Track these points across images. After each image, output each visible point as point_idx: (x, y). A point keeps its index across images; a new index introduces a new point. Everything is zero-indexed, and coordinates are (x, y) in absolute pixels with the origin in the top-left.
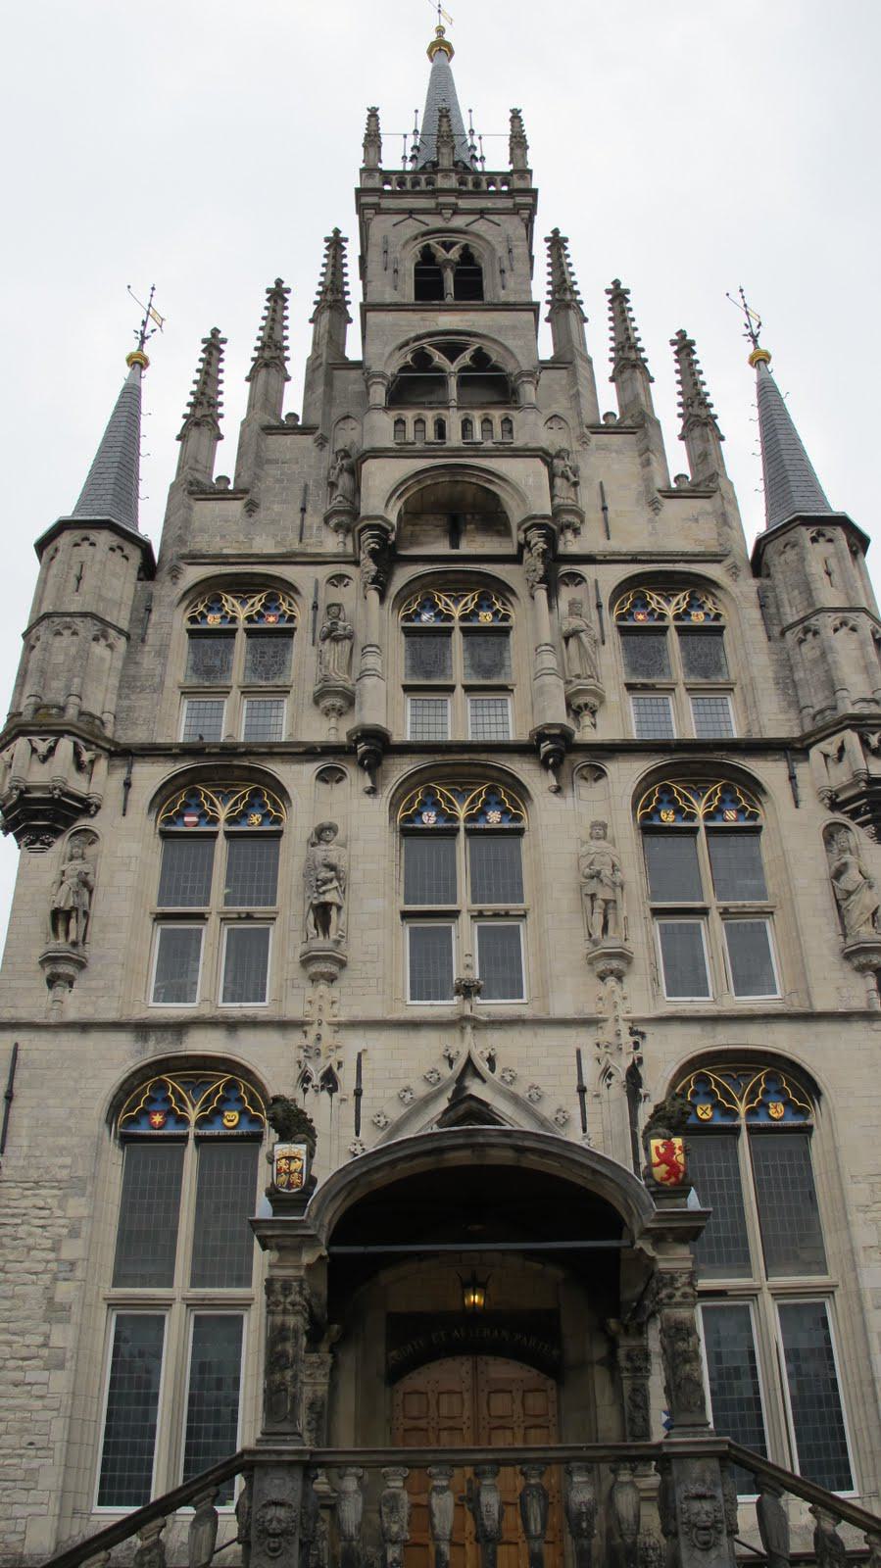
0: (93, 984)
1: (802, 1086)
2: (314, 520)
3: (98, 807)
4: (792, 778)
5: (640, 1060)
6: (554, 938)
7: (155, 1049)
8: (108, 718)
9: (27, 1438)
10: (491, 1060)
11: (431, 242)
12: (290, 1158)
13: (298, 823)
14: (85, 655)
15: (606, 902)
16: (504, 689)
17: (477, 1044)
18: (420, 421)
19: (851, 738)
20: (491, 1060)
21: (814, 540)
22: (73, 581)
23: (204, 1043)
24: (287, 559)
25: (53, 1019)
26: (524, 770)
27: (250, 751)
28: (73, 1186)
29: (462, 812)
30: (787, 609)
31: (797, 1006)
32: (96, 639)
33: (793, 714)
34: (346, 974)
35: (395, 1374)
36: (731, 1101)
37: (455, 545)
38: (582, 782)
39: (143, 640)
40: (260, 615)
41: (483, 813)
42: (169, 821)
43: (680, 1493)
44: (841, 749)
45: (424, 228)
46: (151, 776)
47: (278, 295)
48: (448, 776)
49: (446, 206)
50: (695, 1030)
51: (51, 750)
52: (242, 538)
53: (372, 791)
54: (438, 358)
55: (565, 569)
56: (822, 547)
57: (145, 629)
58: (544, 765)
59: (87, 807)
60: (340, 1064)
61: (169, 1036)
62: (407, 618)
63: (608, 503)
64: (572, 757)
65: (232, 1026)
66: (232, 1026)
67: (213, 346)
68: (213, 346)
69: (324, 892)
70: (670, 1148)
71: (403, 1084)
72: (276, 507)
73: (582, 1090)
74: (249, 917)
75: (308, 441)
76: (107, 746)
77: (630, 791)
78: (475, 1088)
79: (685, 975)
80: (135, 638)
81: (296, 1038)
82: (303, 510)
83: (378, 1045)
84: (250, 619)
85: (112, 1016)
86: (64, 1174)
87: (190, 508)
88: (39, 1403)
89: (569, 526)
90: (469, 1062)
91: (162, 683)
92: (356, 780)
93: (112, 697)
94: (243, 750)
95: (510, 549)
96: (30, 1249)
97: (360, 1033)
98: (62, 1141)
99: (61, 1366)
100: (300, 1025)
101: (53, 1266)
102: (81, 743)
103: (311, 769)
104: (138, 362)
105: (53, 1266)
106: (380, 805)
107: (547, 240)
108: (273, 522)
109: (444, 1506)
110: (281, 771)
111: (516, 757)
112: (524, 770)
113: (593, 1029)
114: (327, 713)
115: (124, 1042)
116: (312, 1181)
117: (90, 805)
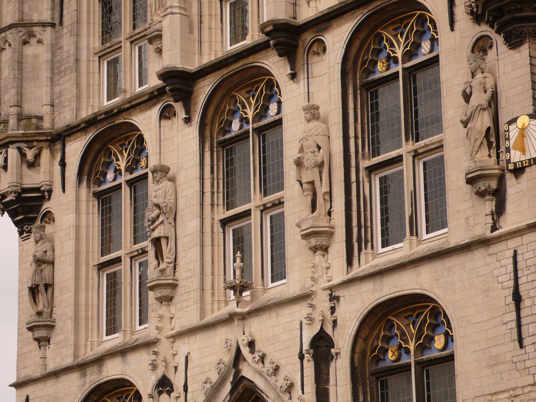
3: (50, 192)
5: (335, 323)
8: (45, 111)
10: (251, 344)
14: (20, 64)
15: (312, 183)
23: (113, 370)
25: (38, 373)
32: (25, 43)
34: (180, 290)
36: (406, 342)
38: (316, 58)
39: (61, 23)
42: (99, 183)
48: (241, 83)
65: (122, 352)
69: (153, 230)
73: (301, 357)
76: (44, 138)
90: (238, 351)
94: (116, 111)
102: (23, 145)
103: (155, 111)
106: (192, 132)
115: (74, 377)
117: (44, 192)
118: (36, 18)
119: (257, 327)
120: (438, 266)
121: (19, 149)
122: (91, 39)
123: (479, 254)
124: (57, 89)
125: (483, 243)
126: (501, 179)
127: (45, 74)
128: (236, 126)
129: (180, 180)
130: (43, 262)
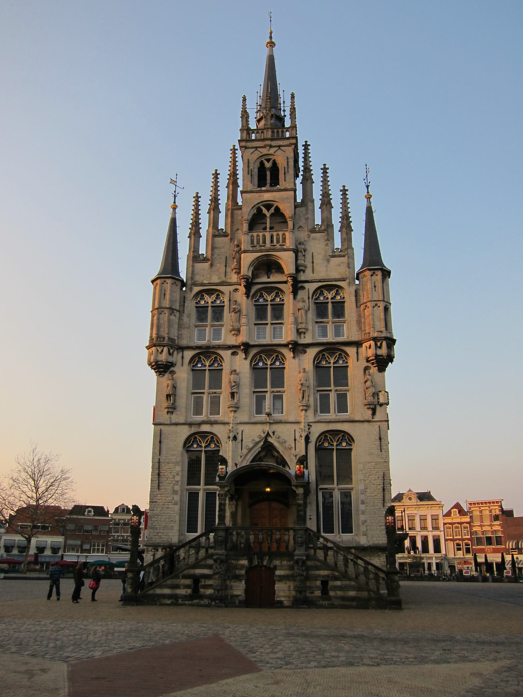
0: (178, 413)
1: (349, 438)
3: (175, 364)
4: (357, 353)
5: (310, 433)
7: (194, 430)
8: (176, 338)
9: (170, 520)
10: (274, 433)
11: (263, 159)
12: (222, 469)
13: (226, 367)
15: (304, 391)
16: (281, 324)
18: (258, 236)
19: (372, 343)
20: (274, 433)
21: (372, 275)
22: (163, 295)
23: (205, 428)
24: (222, 284)
25: (168, 423)
26: (285, 351)
27: (214, 347)
28: (177, 463)
29: (269, 363)
30: (362, 298)
32: (171, 314)
33: (360, 332)
34: (239, 410)
35: (251, 506)
37: (269, 278)
38: (301, 354)
39: (184, 312)
40: (215, 301)
41: (275, 362)
43: (296, 537)
44: (370, 346)
45: (261, 154)
46: (189, 354)
47: (216, 175)
49: (267, 145)
50: (324, 424)
51: (162, 351)
52: (209, 277)
53: (246, 359)
54: (265, 211)
55: (300, 285)
56: (374, 277)
57: (184, 308)
59: (172, 365)
60: (238, 433)
61: (197, 426)
62: (255, 301)
63: (314, 261)
64: (298, 347)
65: (212, 423)
67: (197, 198)
68: (197, 198)
70: (300, 467)
71: (252, 438)
72: (218, 265)
73: (295, 440)
74: (215, 393)
75: (227, 239)
77: (313, 358)
78: (270, 439)
79: (325, 408)
80: (181, 312)
81: (227, 426)
82: (226, 266)
84: (212, 302)
85: (182, 421)
86: (174, 460)
87: (193, 266)
88: (173, 512)
89: (302, 270)
91: (189, 326)
93: (176, 331)
95: (284, 279)
96: (168, 478)
97: (242, 425)
98: (173, 453)
99: (176, 504)
100: (228, 423)
101: (174, 482)
103: (229, 352)
104: (174, 208)
105: (174, 482)
106: (248, 362)
107: (303, 146)
108: (218, 270)
109: (252, 537)
110: (221, 352)
111: (283, 347)
112: (285, 351)
113: (298, 424)
114: (233, 335)
115: (186, 427)
116: (227, 473)
118: (174, 307)
119: (276, 428)
120: (351, 424)
121: (168, 348)
122: (193, 320)
123: (366, 425)
124: (180, 332)
125: (369, 421)
126: (375, 406)
127: (176, 326)
128: (261, 364)
129: (241, 375)
130: (174, 387)
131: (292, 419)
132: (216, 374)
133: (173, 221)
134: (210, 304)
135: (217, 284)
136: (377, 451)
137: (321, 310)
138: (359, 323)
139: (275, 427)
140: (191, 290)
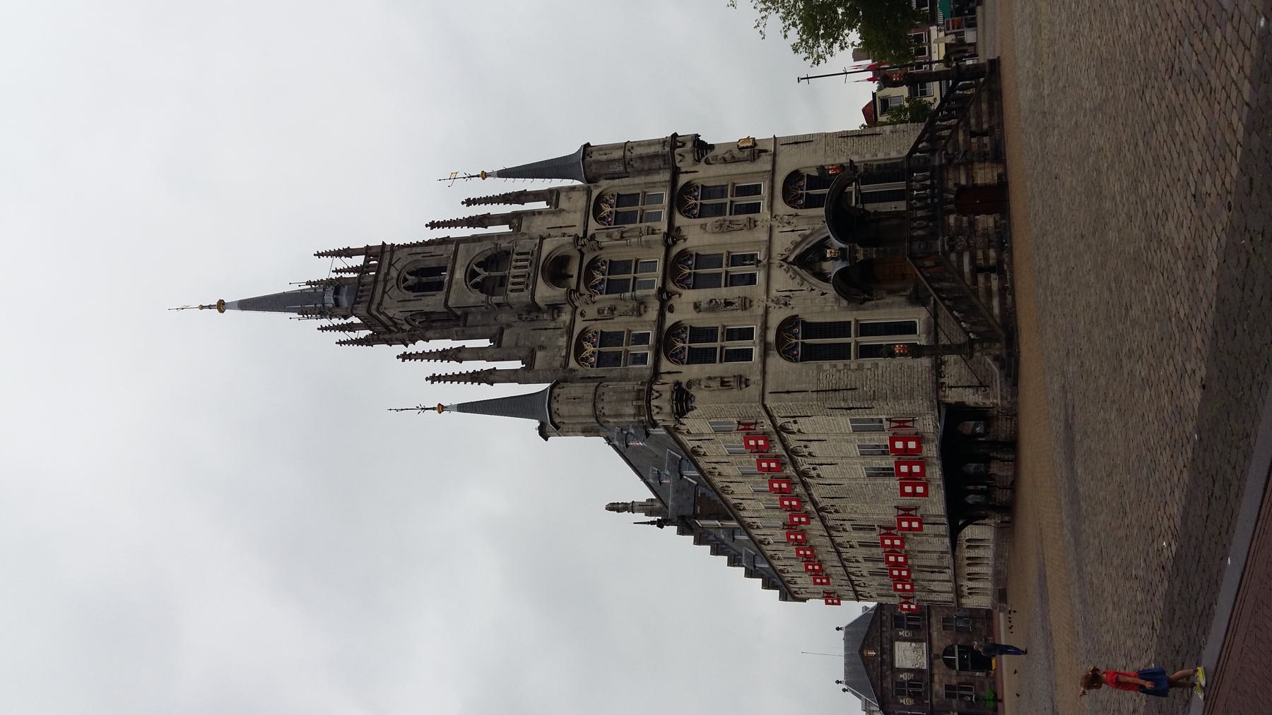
1: (794, 176)
2: (552, 325)
6: (739, 241)
17: (776, 260)
19: (678, 151)
23: (771, 337)
24: (570, 332)
26: (675, 250)
31: (769, 176)
58: (675, 243)
66: (765, 328)
83: (775, 286)
92: (675, 301)
103: (668, 315)
104: (441, 408)
112: (675, 250)
125: (775, 155)
131: (765, 237)
132: (699, 334)
133: (464, 408)
134: (597, 349)
135: (570, 338)
136: (812, 146)
137: (621, 219)
138: (649, 172)
139: (774, 254)
140: (573, 370)
